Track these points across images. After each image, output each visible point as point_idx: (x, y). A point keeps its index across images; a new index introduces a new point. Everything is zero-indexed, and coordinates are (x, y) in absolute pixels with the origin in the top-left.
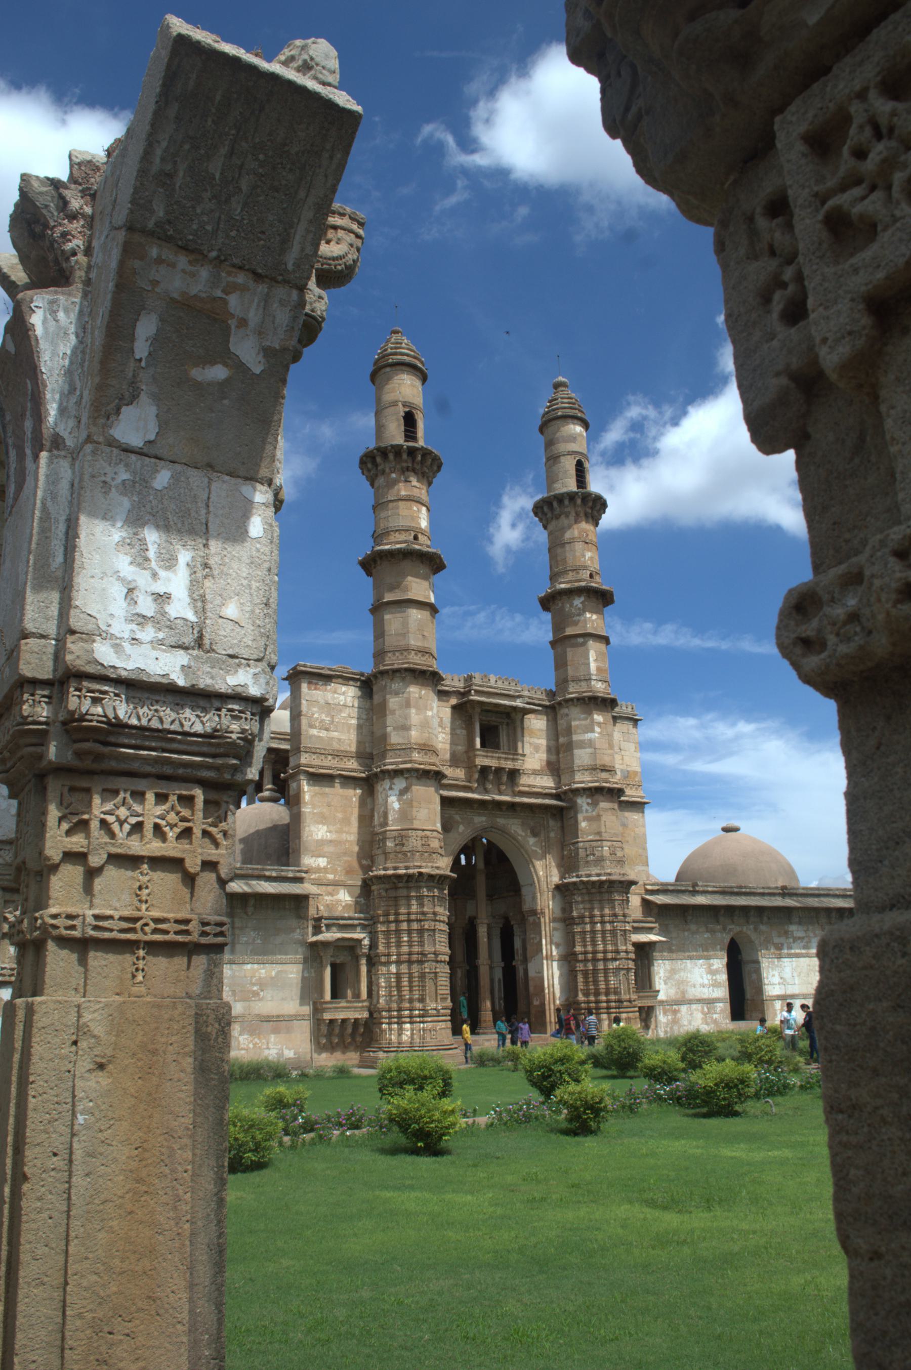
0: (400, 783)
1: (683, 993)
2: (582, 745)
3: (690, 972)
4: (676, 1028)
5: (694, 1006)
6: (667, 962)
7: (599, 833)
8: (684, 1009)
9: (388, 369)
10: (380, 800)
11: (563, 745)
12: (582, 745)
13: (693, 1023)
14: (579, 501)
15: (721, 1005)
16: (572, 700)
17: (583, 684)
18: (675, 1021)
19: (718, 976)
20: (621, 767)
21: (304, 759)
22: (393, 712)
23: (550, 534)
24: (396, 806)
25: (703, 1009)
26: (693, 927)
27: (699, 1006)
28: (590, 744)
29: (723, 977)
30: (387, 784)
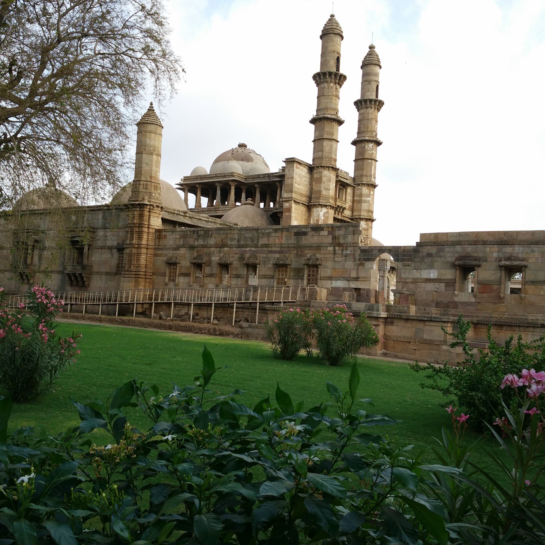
0: (324, 210)
2: (365, 202)
7: (367, 235)
9: (333, 35)
10: (315, 215)
11: (356, 200)
12: (365, 202)
14: (378, 103)
16: (364, 184)
17: (369, 178)
21: (294, 195)
22: (324, 182)
23: (360, 114)
24: (322, 218)
28: (368, 202)
30: (319, 209)
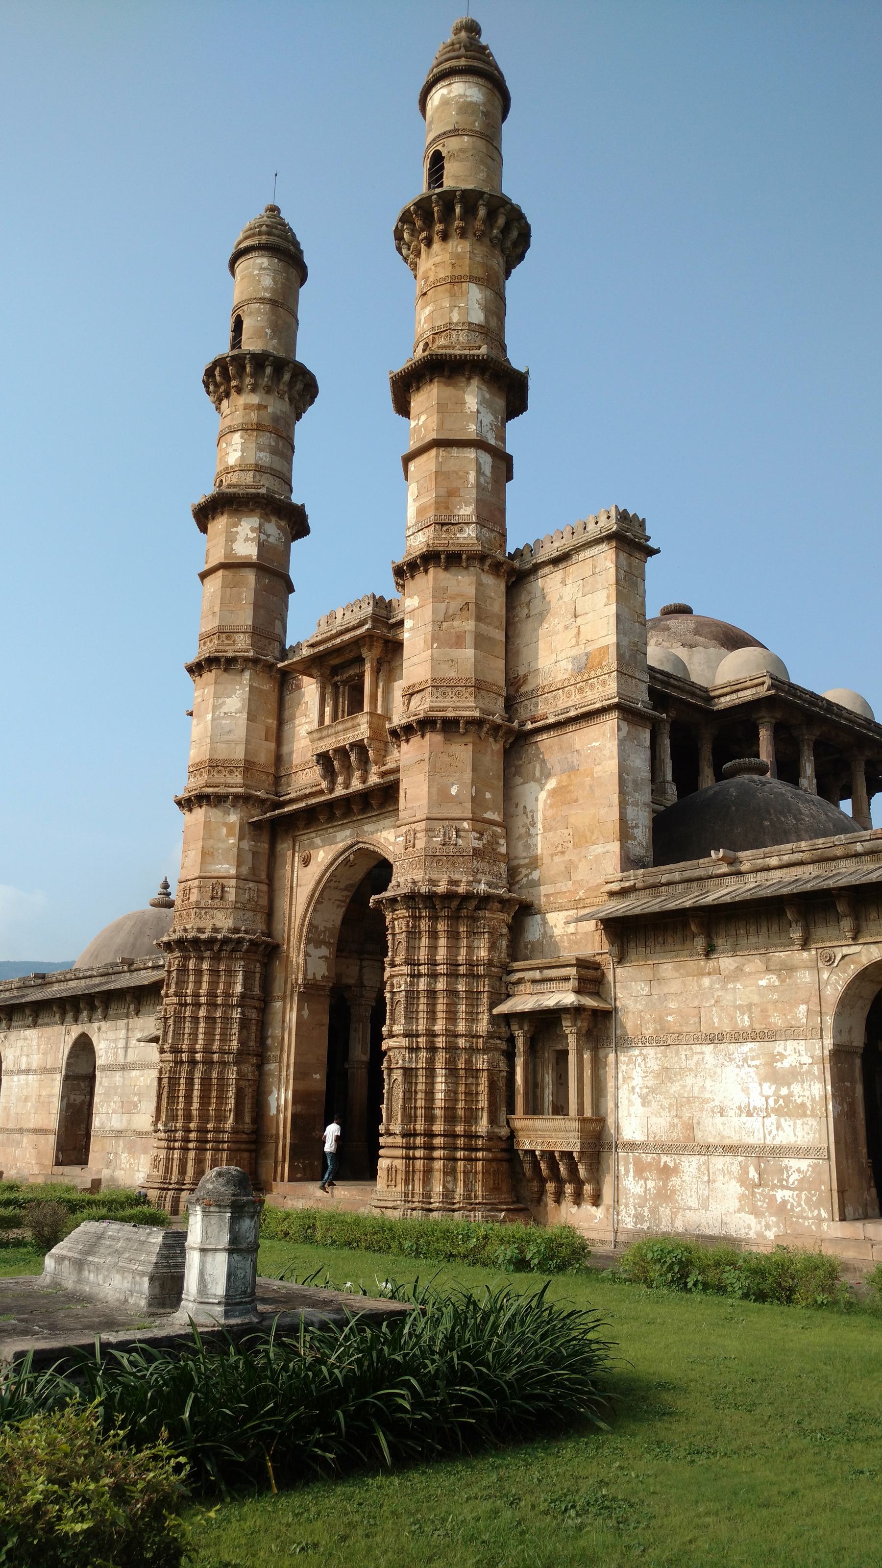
1: (690, 1127)
3: (713, 1076)
4: (665, 1211)
5: (719, 1162)
6: (650, 1052)
8: (690, 1165)
13: (713, 1205)
15: (804, 1164)
18: (665, 1195)
19: (796, 1088)
20: (574, 652)
25: (745, 1170)
26: (726, 962)
27: (733, 1163)
29: (816, 1090)
